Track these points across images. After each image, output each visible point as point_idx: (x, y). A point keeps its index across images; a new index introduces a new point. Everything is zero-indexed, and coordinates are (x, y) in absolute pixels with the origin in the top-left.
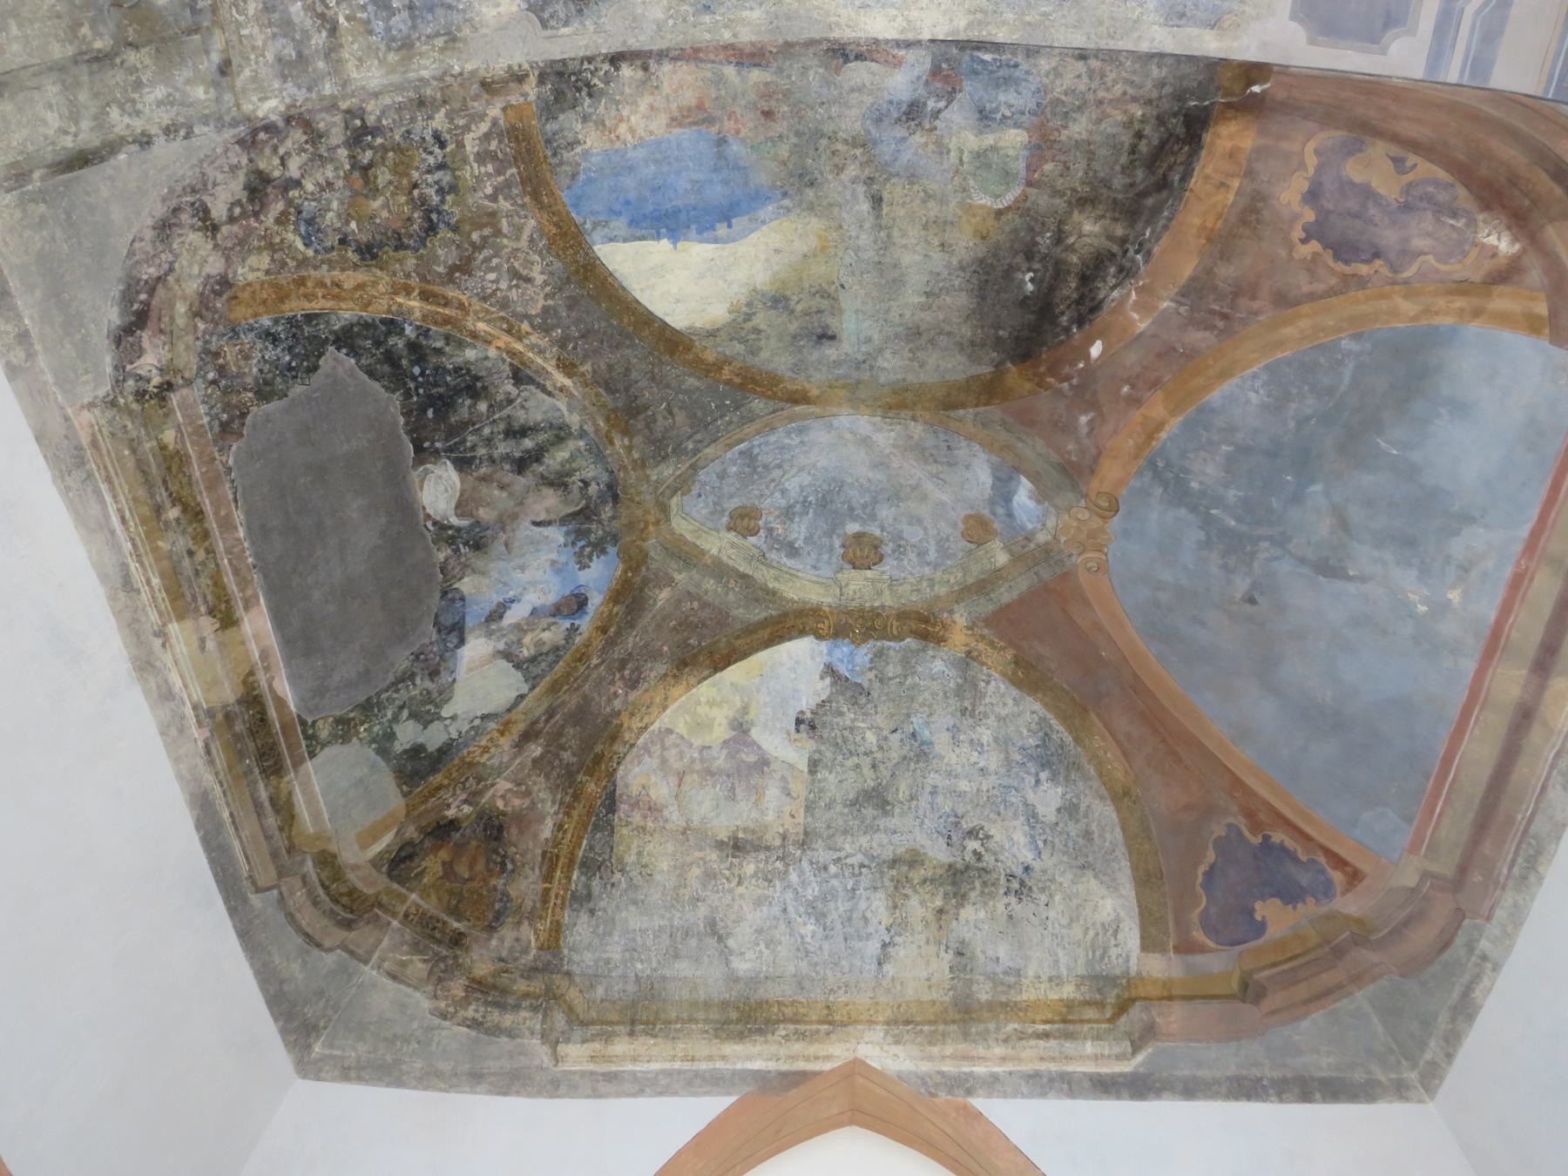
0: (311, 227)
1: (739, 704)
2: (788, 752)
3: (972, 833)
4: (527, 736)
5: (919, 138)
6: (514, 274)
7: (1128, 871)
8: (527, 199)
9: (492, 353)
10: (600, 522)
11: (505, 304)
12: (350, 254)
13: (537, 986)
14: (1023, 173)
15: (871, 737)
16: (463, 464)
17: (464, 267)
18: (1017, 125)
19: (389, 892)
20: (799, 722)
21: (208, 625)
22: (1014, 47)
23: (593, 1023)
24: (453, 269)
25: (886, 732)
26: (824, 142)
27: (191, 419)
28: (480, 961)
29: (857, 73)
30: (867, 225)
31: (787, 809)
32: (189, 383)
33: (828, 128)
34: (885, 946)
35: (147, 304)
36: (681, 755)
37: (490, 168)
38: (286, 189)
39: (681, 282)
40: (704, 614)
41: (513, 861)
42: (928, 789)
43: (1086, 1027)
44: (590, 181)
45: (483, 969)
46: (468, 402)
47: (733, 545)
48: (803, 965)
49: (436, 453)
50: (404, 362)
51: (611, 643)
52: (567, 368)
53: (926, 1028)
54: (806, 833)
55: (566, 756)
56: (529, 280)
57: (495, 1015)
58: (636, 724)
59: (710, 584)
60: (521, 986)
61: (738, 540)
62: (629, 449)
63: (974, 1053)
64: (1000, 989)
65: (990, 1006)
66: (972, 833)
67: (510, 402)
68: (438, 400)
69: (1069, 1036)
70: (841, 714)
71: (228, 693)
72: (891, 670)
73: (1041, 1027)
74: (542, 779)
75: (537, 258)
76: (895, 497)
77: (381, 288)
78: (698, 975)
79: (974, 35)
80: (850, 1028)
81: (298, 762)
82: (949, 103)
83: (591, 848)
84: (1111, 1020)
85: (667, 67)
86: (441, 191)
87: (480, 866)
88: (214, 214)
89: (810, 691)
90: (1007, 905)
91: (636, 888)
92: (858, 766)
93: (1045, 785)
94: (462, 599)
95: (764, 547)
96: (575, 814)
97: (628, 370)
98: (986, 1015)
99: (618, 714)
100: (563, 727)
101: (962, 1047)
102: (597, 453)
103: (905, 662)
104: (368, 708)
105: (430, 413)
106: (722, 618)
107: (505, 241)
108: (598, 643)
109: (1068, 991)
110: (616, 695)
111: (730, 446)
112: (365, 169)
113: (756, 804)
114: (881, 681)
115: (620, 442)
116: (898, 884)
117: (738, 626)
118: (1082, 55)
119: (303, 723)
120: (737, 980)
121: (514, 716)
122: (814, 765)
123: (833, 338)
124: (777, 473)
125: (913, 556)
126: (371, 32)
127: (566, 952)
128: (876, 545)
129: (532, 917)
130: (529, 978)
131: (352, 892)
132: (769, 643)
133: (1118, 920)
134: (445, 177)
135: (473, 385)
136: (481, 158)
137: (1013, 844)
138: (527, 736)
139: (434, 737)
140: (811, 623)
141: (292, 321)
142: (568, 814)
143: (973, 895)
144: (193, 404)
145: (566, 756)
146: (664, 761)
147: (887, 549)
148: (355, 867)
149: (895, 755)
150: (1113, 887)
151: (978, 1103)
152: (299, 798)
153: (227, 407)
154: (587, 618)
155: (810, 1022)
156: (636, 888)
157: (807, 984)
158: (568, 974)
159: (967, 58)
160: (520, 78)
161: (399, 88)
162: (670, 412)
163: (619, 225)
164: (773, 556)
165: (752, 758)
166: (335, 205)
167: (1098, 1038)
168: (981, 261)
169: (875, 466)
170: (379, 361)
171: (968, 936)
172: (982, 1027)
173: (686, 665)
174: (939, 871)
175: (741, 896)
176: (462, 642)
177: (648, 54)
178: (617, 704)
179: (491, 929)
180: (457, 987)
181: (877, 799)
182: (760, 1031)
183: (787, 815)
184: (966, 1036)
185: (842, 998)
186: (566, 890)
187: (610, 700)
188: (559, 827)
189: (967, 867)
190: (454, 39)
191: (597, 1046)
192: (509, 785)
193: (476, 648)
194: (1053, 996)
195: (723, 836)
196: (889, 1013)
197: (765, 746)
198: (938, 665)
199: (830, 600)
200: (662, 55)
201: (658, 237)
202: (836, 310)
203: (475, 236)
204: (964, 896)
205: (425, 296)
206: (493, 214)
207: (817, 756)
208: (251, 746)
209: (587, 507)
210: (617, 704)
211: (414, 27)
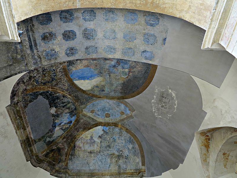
0: (37, 82)
3: (121, 151)
4: (64, 138)
9: (60, 94)
11: (62, 88)
13: (64, 171)
17: (57, 84)
19: (45, 159)
20: (99, 137)
21: (22, 130)
22: (127, 60)
23: (72, 176)
24: (55, 85)
27: (21, 106)
28: (57, 168)
29: (108, 62)
32: (21, 102)
35: (15, 93)
37: (61, 73)
38: (34, 78)
39: (85, 85)
45: (57, 168)
49: (53, 106)
52: (70, 95)
57: (59, 175)
58: (78, 137)
59: (88, 119)
60: (62, 171)
65: (123, 173)
66: (121, 151)
67: (62, 99)
68: (53, 100)
71: (25, 138)
73: (129, 176)
76: (112, 109)
77: (46, 88)
78: (86, 169)
81: (33, 145)
85: (83, 61)
86: (54, 76)
87: (57, 155)
88: (25, 81)
91: (78, 158)
93: (130, 145)
102: (74, 105)
103: (113, 129)
104: (43, 137)
106: (89, 123)
108: (73, 127)
109: (132, 171)
111: (91, 103)
112: (44, 74)
116: (112, 157)
118: (135, 62)
119: (34, 140)
120: (91, 170)
121: (62, 136)
122: (101, 142)
126: (46, 59)
129: (64, 162)
131: (40, 159)
133: (139, 162)
134: (55, 74)
135: (58, 98)
136: (59, 72)
137: (126, 153)
138: (64, 138)
139: (51, 140)
140: (101, 124)
144: (21, 104)
145: (69, 141)
146: (82, 141)
147: (111, 115)
148: (41, 156)
150: (138, 158)
153: (25, 104)
160: (65, 63)
163: (77, 79)
164: (96, 116)
169: (109, 105)
176: (55, 128)
180: (54, 171)
181: (109, 146)
188: (68, 150)
193: (57, 128)
198: (117, 130)
200: (83, 59)
201: (82, 80)
205: (51, 88)
206: (61, 78)
208: (27, 144)
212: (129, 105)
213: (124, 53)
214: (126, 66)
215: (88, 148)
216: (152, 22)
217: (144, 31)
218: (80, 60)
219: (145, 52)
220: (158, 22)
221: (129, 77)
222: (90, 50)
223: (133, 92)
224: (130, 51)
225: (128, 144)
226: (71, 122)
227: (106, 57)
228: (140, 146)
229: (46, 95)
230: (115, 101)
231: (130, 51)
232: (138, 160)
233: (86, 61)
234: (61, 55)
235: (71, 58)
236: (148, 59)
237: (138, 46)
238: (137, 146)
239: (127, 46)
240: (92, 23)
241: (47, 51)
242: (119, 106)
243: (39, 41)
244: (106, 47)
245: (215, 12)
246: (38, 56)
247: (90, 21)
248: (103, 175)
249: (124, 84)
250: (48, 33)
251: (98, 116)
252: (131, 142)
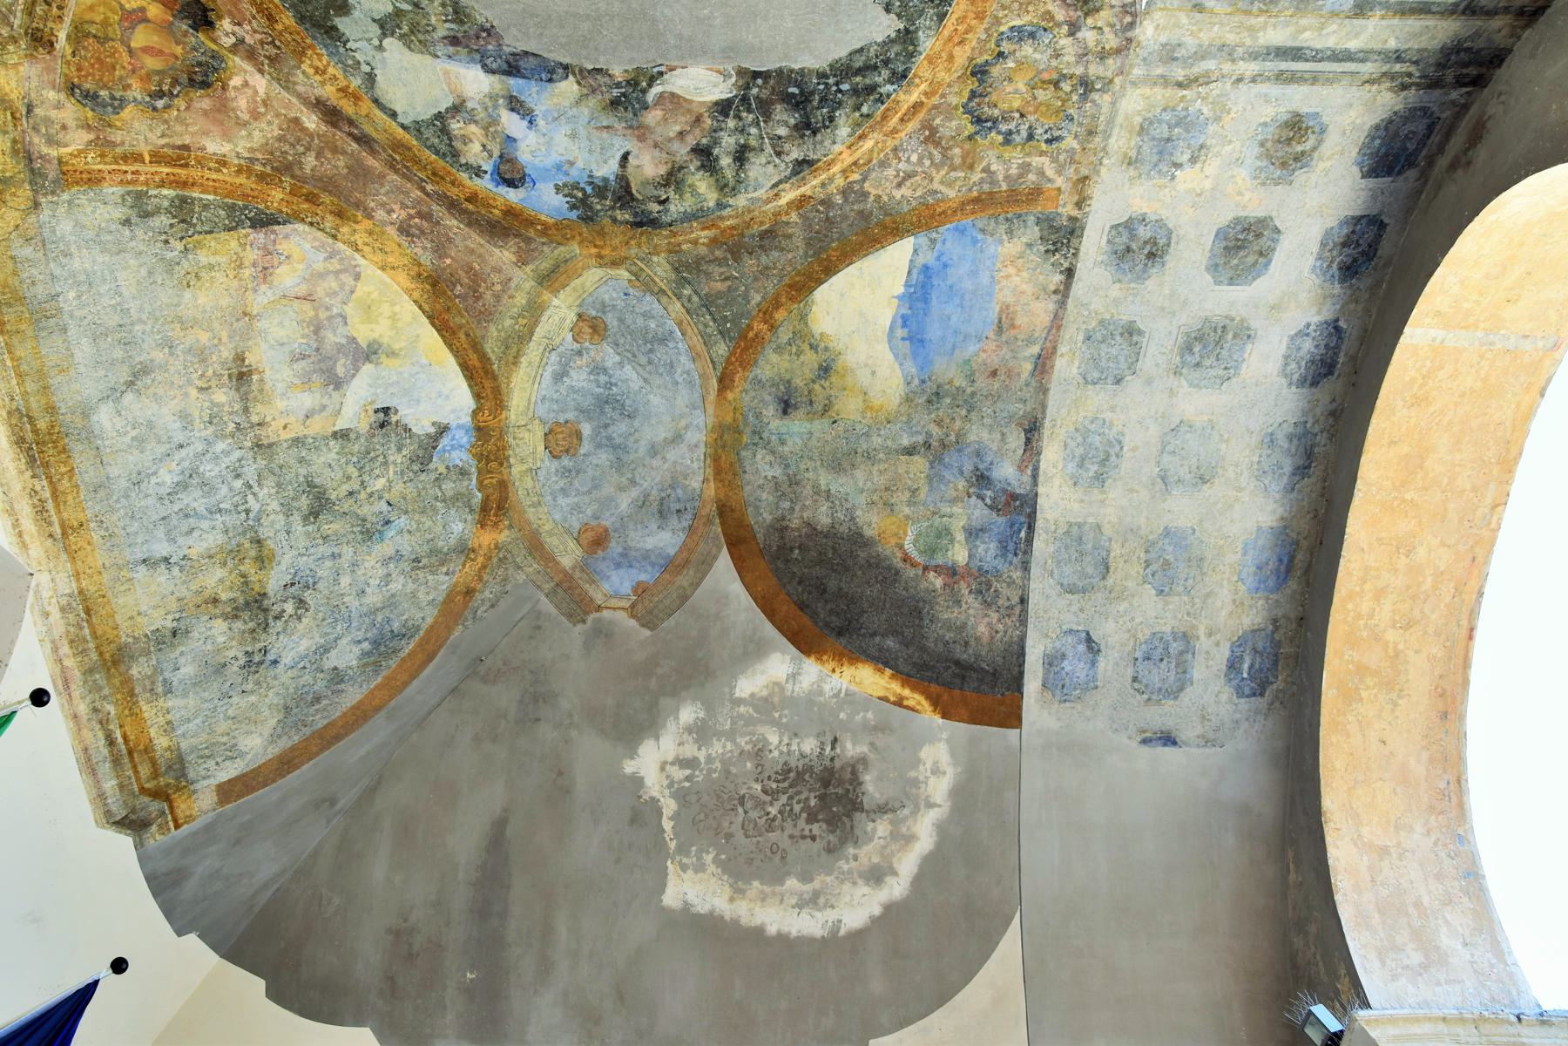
1: (396, 347)
2: (353, 408)
3: (301, 603)
5: (962, 484)
6: (909, 176)
7: (290, 744)
8: (975, 194)
9: (837, 148)
10: (613, 208)
11: (883, 164)
12: (986, 57)
14: (934, 563)
15: (380, 483)
18: (970, 556)
20: (386, 410)
22: (1028, 550)
25: (387, 496)
26: (964, 412)
29: (1016, 440)
30: (889, 443)
31: (292, 419)
33: (973, 416)
34: (166, 560)
36: (335, 294)
40: (488, 296)
41: (167, 107)
42: (336, 550)
43: (130, 773)
44: (975, 242)
46: (792, 121)
47: (564, 319)
48: (123, 483)
50: (858, 79)
51: (452, 205)
52: (801, 202)
53: (87, 631)
54: (270, 446)
55: (310, 161)
56: (899, 185)
58: (360, 238)
59: (520, 300)
61: (568, 324)
62: (695, 242)
63: (73, 687)
64: (147, 683)
65: (127, 681)
69: (116, 762)
70: (399, 450)
73: (118, 735)
74: (277, 132)
75: (919, 193)
76: (619, 465)
79: (1039, 524)
80: (64, 556)
82: (991, 507)
83: (206, 207)
84: (143, 790)
85: (1051, 306)
87: (151, 63)
89: (418, 418)
90: (236, 658)
91: (170, 272)
92: (349, 478)
93: (356, 650)
94: (550, 80)
95: (562, 349)
96: (242, 180)
97: (782, 250)
98: (116, 682)
99: (370, 217)
100: (344, 153)
101: (77, 675)
103: (457, 497)
105: (796, 91)
106: (486, 316)
107: (943, 172)
108: (453, 192)
109: (161, 743)
110: (389, 212)
111: (679, 324)
112: (1056, 84)
113: (292, 385)
114: (437, 479)
115: (704, 236)
116: (236, 554)
117: (479, 333)
118: (1023, 601)
120: (86, 415)
121: (366, 106)
122: (342, 435)
123: (785, 412)
124: (643, 360)
125: (561, 484)
127: (65, 196)
129: (102, 145)
130: (15, 152)
132: (465, 368)
133: (242, 755)
137: (293, 644)
142: (239, 171)
143: (239, 625)
145: (310, 161)
146: (322, 276)
147: (566, 461)
149: (366, 511)
154: (491, 186)
155: (59, 512)
156: (170, 272)
157: (101, 494)
158: (36, 205)
159: (1023, 519)
160: (1079, 205)
161: (1111, 121)
162: (726, 279)
163: (926, 258)
164: (554, 357)
165: (340, 370)
166: (1038, 56)
167: (121, 787)
168: (861, 535)
170: (868, 59)
171: (195, 634)
172: (103, 683)
173: (434, 285)
174: (257, 588)
175: (186, 394)
177: (1066, 296)
178: (380, 214)
181: (319, 505)
182: (32, 461)
183: (283, 422)
184: (90, 671)
185: (96, 537)
186: (146, 183)
187: (383, 205)
188: (222, 162)
189: (266, 610)
190: (1129, 164)
192: (261, 91)
194: (153, 732)
195: (250, 359)
196: (92, 589)
197: (356, 382)
198: (459, 526)
199: (513, 417)
200: (1062, 304)
201: (907, 285)
202: (812, 416)
203: (957, 151)
204: (236, 617)
205: (917, 106)
207: (352, 436)
209: (633, 199)
210: (380, 214)
211: (1154, 139)
212: (683, 580)
213: (1074, 536)
214: (988, 550)
215: (275, 345)
216: (1246, 666)
217: (1202, 632)
219: (1090, 648)
220: (1247, 691)
221: (911, 572)
222: (1118, 347)
223: (802, 607)
224: (1090, 570)
225: (360, 635)
227: (1046, 432)
228: (360, 715)
230: (698, 479)
231: (1090, 570)
232: (256, 746)
235: (1093, 244)
236: (1047, 672)
237: (1123, 606)
238: (353, 695)
239: (1116, 550)
241: (1211, 129)
242: (662, 514)
243: (1299, 98)
244: (1112, 434)
245: (1511, 1024)
246: (1207, 74)
248: (67, 537)
249: (858, 539)
250: (1314, 149)
251: (549, 369)
252: (381, 646)
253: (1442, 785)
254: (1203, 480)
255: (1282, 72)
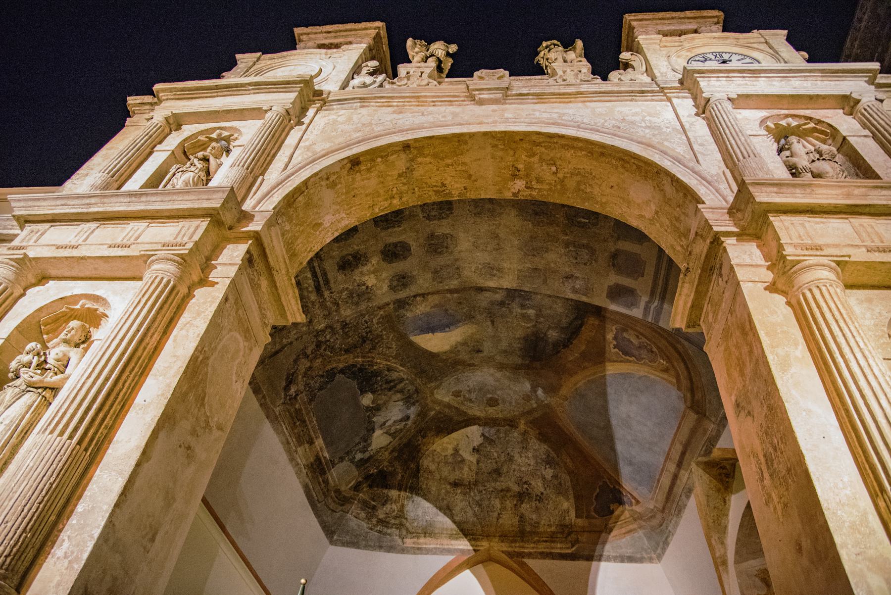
2: (471, 458)
3: (526, 483)
5: (504, 309)
13: (397, 522)
15: (495, 454)
16: (373, 392)
17: (374, 348)
21: (307, 446)
22: (531, 292)
29: (487, 294)
39: (434, 343)
45: (381, 516)
49: (366, 392)
58: (425, 448)
60: (393, 521)
66: (526, 483)
68: (367, 379)
69: (552, 542)
71: (312, 460)
72: (501, 435)
81: (329, 470)
86: (367, 333)
89: (477, 441)
102: (412, 383)
106: (451, 419)
109: (553, 529)
115: (418, 380)
118: (550, 296)
128: (497, 400)
129: (396, 502)
131: (344, 497)
135: (376, 374)
137: (538, 486)
138: (392, 451)
139: (367, 455)
141: (328, 371)
144: (303, 397)
146: (434, 459)
150: (567, 499)
151: (526, 560)
152: (330, 478)
179: (384, 505)
180: (374, 521)
181: (497, 472)
184: (523, 541)
188: (403, 476)
191: (415, 540)
193: (378, 433)
195: (451, 481)
200: (428, 294)
218: (423, 295)
226: (408, 418)
229: (351, 371)
233: (435, 296)
234: (379, 292)
235: (402, 294)
240: (444, 222)
241: (351, 288)
244: (480, 267)
247: (439, 219)
249: (526, 338)
253: (635, 167)
254: (497, 236)
255: (325, 284)
